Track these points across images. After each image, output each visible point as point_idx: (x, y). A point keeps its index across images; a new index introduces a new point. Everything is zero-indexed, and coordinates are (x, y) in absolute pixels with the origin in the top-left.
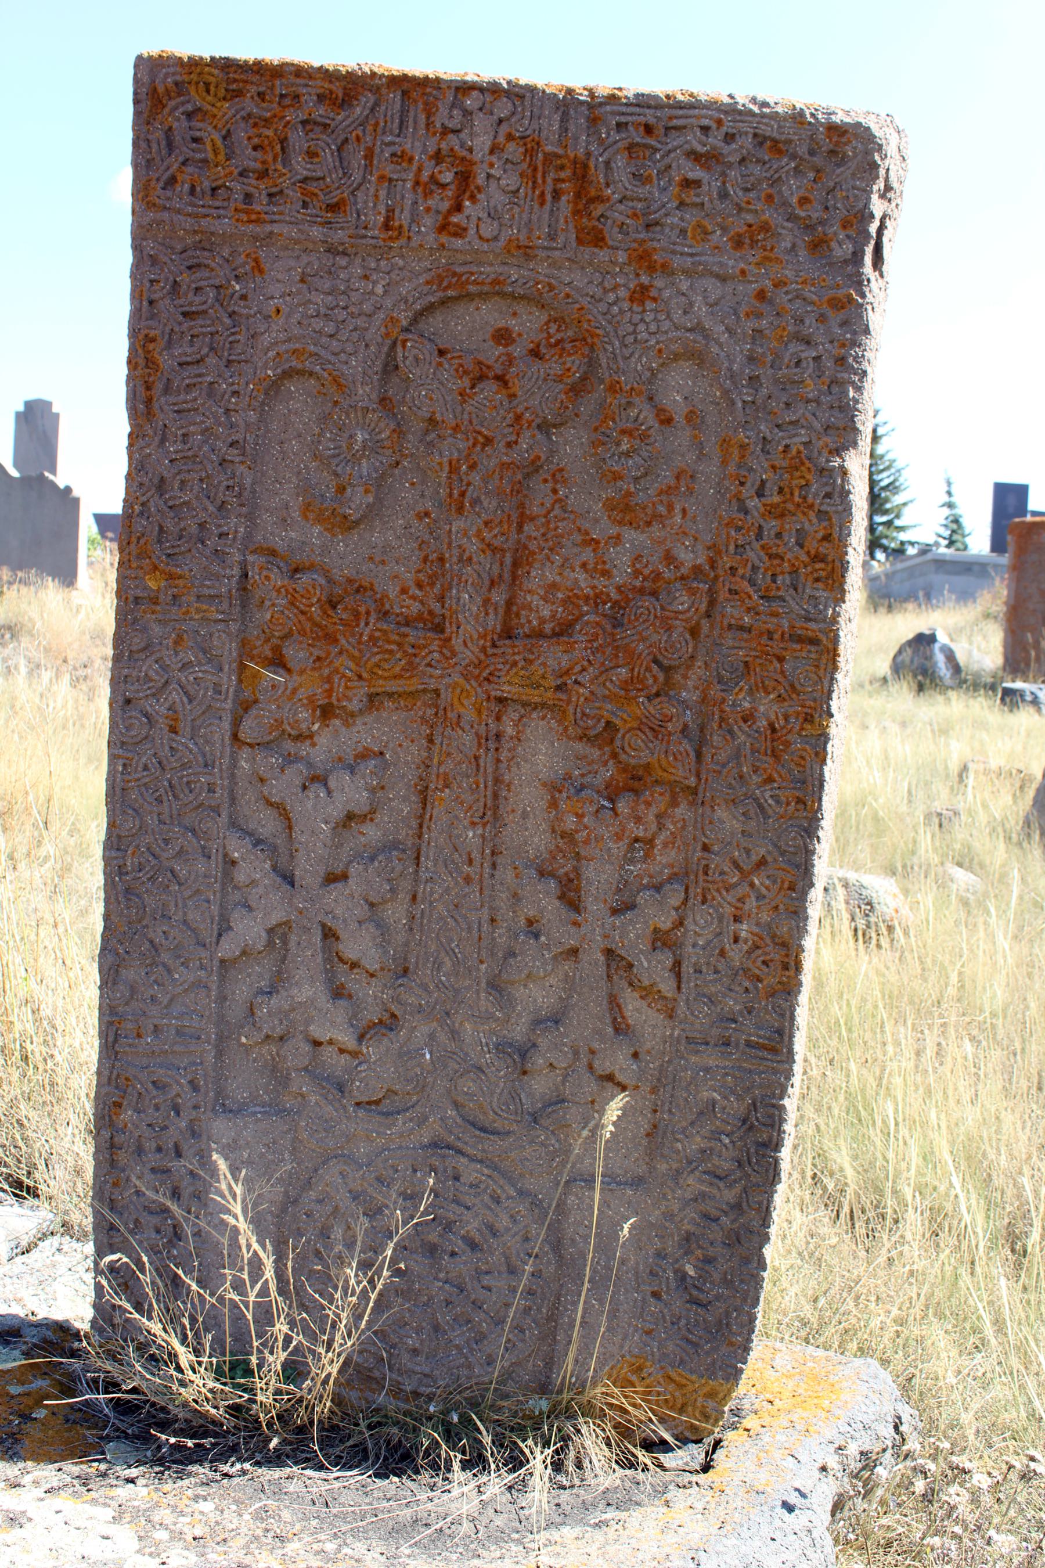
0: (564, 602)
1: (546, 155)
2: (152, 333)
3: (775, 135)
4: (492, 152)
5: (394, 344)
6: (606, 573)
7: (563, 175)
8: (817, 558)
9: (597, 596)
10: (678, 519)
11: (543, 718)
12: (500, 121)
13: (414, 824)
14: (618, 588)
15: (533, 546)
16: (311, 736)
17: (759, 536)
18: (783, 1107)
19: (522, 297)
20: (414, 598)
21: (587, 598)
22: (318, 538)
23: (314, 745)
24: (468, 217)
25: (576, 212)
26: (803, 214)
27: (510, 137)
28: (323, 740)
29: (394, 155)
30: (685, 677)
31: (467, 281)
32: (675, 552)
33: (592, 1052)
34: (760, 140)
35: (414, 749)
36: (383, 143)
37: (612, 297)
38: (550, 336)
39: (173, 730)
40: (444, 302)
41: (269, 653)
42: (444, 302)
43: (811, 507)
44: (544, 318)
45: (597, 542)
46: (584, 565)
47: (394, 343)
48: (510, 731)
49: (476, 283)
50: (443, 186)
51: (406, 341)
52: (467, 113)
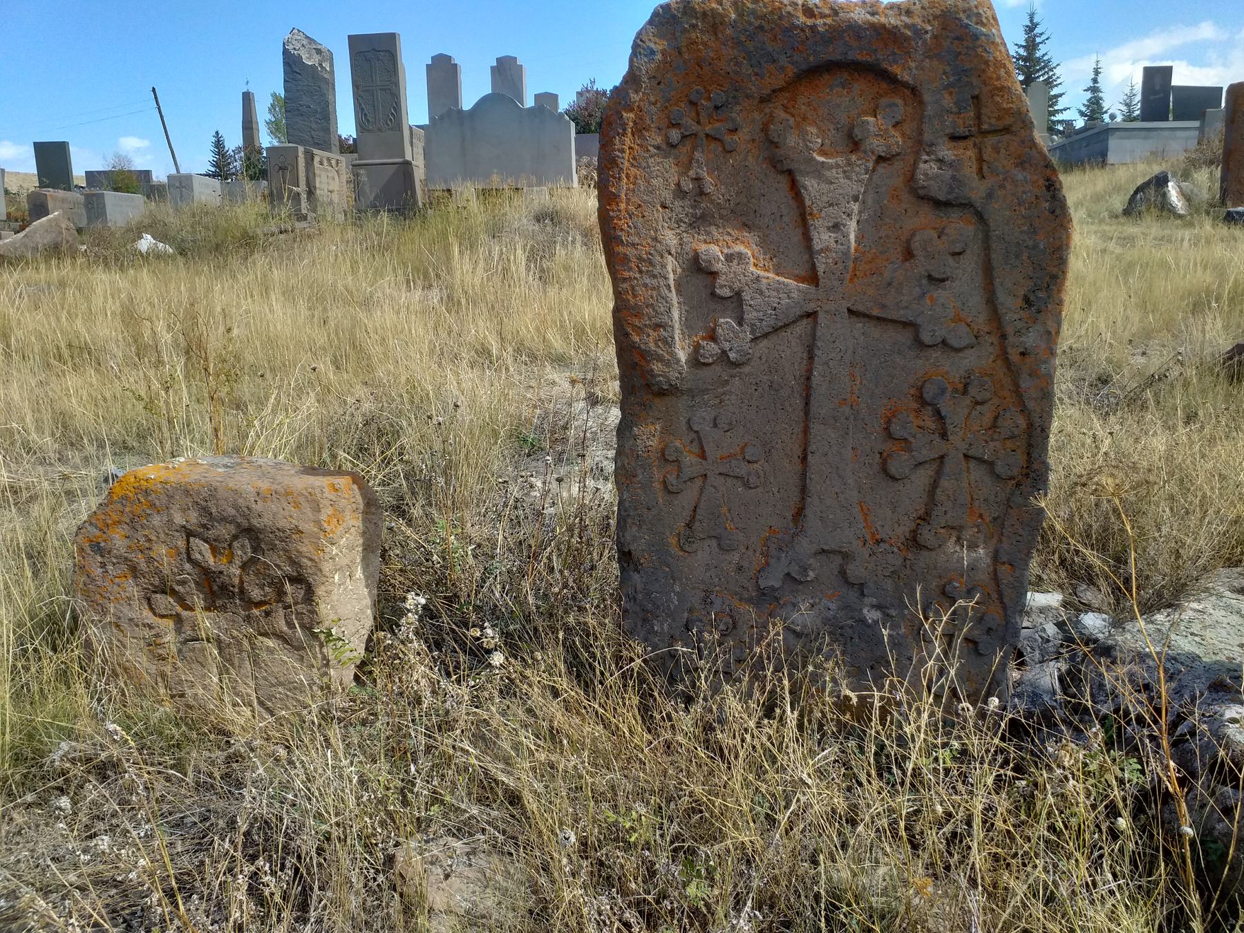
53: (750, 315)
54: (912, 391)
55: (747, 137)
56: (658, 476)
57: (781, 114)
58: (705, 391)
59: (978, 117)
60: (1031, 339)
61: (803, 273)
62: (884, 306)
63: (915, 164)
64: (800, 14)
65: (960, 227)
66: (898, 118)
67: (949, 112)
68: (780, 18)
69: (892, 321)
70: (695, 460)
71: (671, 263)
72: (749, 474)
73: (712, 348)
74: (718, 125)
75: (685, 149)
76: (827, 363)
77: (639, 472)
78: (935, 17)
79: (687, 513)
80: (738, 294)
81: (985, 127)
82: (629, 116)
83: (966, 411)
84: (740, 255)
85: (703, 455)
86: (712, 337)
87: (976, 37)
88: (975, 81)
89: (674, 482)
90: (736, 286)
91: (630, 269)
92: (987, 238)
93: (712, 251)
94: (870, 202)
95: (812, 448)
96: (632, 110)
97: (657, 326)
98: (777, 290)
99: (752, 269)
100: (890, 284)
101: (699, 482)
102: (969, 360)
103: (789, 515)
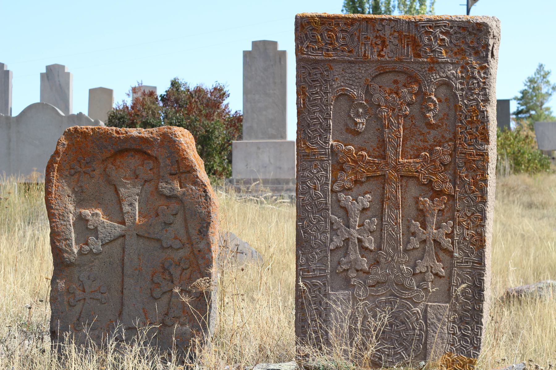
0: (417, 150)
6: (427, 142)
7: (409, 40)
8: (482, 134)
10: (445, 126)
14: (430, 145)
15: (407, 136)
17: (466, 129)
18: (483, 280)
19: (400, 72)
20: (377, 151)
25: (413, 49)
27: (395, 31)
28: (355, 190)
30: (449, 167)
32: (444, 135)
33: (432, 267)
34: (459, 27)
35: (379, 190)
37: (424, 70)
39: (315, 189)
40: (380, 74)
41: (339, 168)
42: (380, 74)
43: (479, 121)
44: (406, 77)
46: (421, 140)
48: (404, 184)
50: (378, 45)
52: (383, 26)
53: (101, 236)
54: (161, 265)
55: (99, 173)
56: (66, 299)
57: (110, 165)
58: (85, 265)
59: (179, 167)
60: (202, 246)
61: (120, 221)
62: (149, 233)
63: (158, 184)
64: (114, 133)
65: (174, 206)
66: (151, 167)
67: (169, 165)
68: (108, 134)
69: (153, 239)
70: (81, 292)
71: (71, 216)
72: (102, 298)
73: (87, 248)
74: (88, 169)
75: (76, 176)
76: (129, 254)
77: (59, 297)
78: (161, 135)
79: (77, 315)
80: (96, 228)
81: (181, 171)
82: (56, 166)
83: (179, 272)
84: (97, 213)
85: (84, 291)
86: (87, 244)
87: (175, 141)
88: (176, 156)
89: (73, 302)
90: (96, 225)
91: (56, 218)
92: (184, 210)
93: (87, 212)
94: (143, 196)
95: (125, 287)
96: (57, 163)
97: (66, 240)
98: (111, 227)
99: (101, 219)
100: (151, 225)
101: (82, 302)
102: (181, 253)
103: (117, 314)
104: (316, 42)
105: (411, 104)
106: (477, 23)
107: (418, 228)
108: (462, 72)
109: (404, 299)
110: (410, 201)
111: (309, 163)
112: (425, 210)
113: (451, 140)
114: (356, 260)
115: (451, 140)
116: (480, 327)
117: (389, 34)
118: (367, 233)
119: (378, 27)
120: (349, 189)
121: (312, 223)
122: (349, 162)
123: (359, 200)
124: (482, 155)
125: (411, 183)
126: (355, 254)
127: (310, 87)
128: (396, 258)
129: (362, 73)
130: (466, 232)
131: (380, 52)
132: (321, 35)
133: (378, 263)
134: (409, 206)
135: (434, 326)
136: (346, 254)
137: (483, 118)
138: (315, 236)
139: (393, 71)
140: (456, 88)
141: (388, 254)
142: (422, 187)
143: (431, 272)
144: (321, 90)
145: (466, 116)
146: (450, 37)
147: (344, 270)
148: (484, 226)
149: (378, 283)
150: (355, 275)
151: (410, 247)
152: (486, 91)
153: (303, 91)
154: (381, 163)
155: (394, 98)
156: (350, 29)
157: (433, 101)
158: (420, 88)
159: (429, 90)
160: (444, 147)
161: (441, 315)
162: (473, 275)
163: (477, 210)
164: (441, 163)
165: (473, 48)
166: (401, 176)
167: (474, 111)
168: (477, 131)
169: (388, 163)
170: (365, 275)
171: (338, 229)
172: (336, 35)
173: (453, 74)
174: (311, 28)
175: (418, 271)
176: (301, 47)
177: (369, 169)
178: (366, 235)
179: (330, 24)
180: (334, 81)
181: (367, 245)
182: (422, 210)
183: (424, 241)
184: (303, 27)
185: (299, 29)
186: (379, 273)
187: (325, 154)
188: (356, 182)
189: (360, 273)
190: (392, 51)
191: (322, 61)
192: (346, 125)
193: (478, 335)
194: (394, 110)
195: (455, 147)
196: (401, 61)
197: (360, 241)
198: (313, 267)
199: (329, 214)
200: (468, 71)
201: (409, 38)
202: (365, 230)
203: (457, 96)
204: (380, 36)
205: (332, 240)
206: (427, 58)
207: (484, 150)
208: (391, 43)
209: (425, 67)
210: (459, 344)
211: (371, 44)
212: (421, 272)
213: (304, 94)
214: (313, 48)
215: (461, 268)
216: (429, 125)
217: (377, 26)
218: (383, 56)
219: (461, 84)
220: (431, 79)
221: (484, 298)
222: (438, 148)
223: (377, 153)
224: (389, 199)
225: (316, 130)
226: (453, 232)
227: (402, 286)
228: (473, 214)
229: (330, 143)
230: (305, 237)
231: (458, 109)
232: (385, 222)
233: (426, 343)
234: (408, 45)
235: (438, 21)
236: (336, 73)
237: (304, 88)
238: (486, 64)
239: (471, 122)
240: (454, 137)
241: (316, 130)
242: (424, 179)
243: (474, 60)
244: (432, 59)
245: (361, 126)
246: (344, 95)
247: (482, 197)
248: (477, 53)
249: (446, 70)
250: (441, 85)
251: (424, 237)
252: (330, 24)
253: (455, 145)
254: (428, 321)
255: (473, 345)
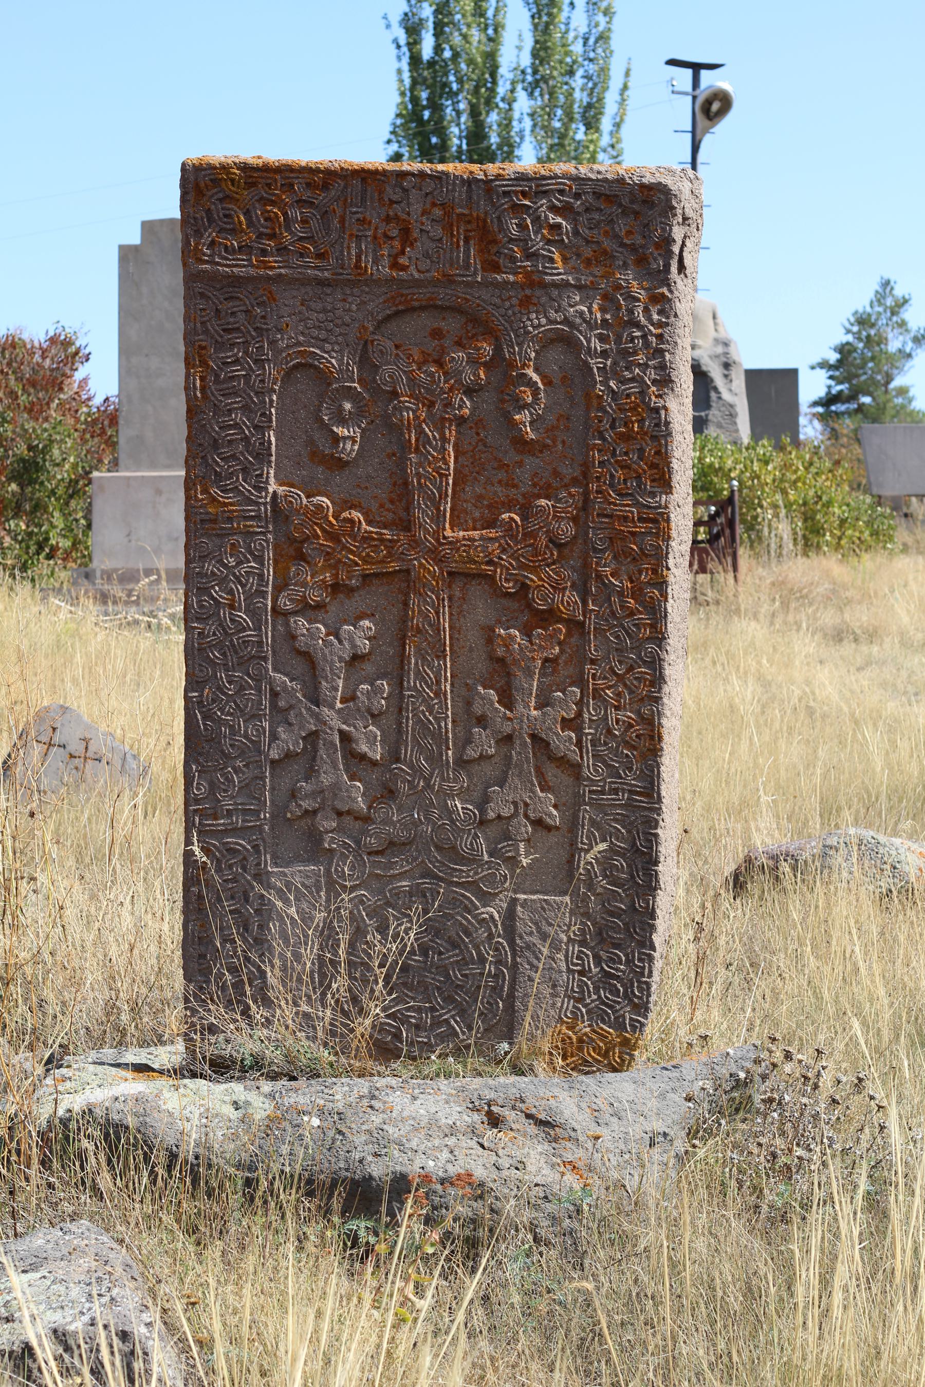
0: (489, 507)
1: (458, 215)
2: (204, 344)
3: (608, 193)
4: (422, 215)
5: (366, 342)
6: (515, 486)
7: (469, 227)
8: (653, 466)
9: (510, 501)
10: (560, 447)
11: (480, 584)
12: (427, 194)
13: (397, 661)
14: (523, 495)
15: (466, 471)
16: (324, 606)
17: (614, 454)
18: (656, 836)
20: (388, 510)
21: (503, 503)
22: (322, 474)
23: (327, 612)
24: (410, 258)
25: (481, 251)
26: (629, 242)
27: (434, 205)
28: (332, 608)
29: (358, 220)
30: (572, 551)
31: (412, 300)
32: (559, 469)
33: (526, 805)
34: (597, 195)
36: (351, 212)
37: (507, 304)
38: (468, 332)
39: (232, 607)
40: (397, 313)
42: (397, 313)
43: (646, 433)
44: (463, 320)
45: (508, 466)
46: (500, 482)
47: (366, 342)
48: (458, 594)
49: (416, 300)
50: (392, 238)
51: (372, 341)
52: (405, 190)
104: (233, 231)
105: (475, 391)
106: (642, 186)
107: (492, 704)
108: (603, 310)
109: (458, 884)
110: (473, 637)
111: (217, 541)
112: (509, 660)
113: (575, 481)
114: (336, 787)
115: (575, 481)
116: (649, 955)
117: (419, 212)
118: (363, 717)
119: (391, 193)
120: (320, 606)
121: (225, 694)
122: (318, 537)
123: (343, 635)
124: (655, 521)
125: (476, 590)
126: (332, 772)
127: (220, 346)
128: (436, 781)
129: (350, 310)
130: (612, 714)
131: (396, 257)
132: (247, 213)
133: (390, 793)
134: (471, 650)
135: (534, 953)
136: (311, 773)
137: (658, 425)
138: (232, 727)
139: (430, 307)
140: (589, 348)
141: (417, 771)
142: (504, 601)
143: (526, 816)
144: (246, 353)
145: (614, 420)
146: (575, 220)
147: (307, 811)
148: (658, 700)
149: (392, 846)
150: (334, 825)
151: (471, 753)
152: (664, 357)
153: (200, 356)
154: (398, 541)
155: (432, 375)
156: (321, 198)
157: (531, 384)
158: (498, 349)
159: (520, 354)
160: (559, 501)
161: (551, 925)
162: (631, 823)
163: (641, 659)
164: (551, 541)
165: (633, 248)
166: (450, 574)
167: (634, 409)
168: (641, 458)
169: (415, 541)
170: (358, 824)
171: (291, 707)
172: (285, 214)
173: (581, 313)
174: (221, 195)
175: (491, 815)
176: (197, 244)
177: (368, 555)
178: (360, 724)
179: (269, 185)
180: (280, 330)
181: (364, 748)
182: (501, 661)
183: (507, 740)
184: (199, 192)
185: (191, 197)
186: (393, 819)
187: (257, 517)
188: (336, 588)
189: (347, 819)
190: (427, 255)
191: (250, 279)
192: (311, 442)
193: (642, 975)
194: (432, 404)
195: (586, 500)
196: (450, 280)
197: (345, 738)
198: (228, 804)
199: (267, 670)
200: (619, 307)
201: (469, 222)
202: (359, 710)
203: (592, 369)
204: (397, 217)
205: (274, 737)
206: (515, 274)
207: (660, 507)
208: (425, 236)
209: (510, 298)
210: (594, 997)
211: (375, 237)
212: (499, 817)
213: (204, 363)
214: (226, 247)
215: (599, 807)
216: (520, 443)
217: (389, 190)
218: (404, 268)
219: (602, 339)
220: (525, 327)
221: (657, 881)
222: (543, 502)
223: (390, 516)
224: (419, 631)
225: (234, 457)
226: (579, 714)
227: (453, 853)
228: (631, 669)
229: (271, 490)
230: (206, 729)
231: (595, 402)
232: (409, 690)
233: (511, 996)
234: (467, 240)
235: (544, 178)
236: (285, 311)
237: (204, 348)
238: (665, 290)
239: (627, 437)
240: (585, 474)
241: (234, 457)
242: (507, 580)
243: (634, 279)
244: (527, 275)
245: (348, 446)
246: (306, 368)
247: (653, 626)
248: (642, 261)
249: (565, 303)
250: (552, 341)
251: (507, 728)
252: (269, 185)
253: (586, 494)
254: (518, 941)
255: (631, 1001)
